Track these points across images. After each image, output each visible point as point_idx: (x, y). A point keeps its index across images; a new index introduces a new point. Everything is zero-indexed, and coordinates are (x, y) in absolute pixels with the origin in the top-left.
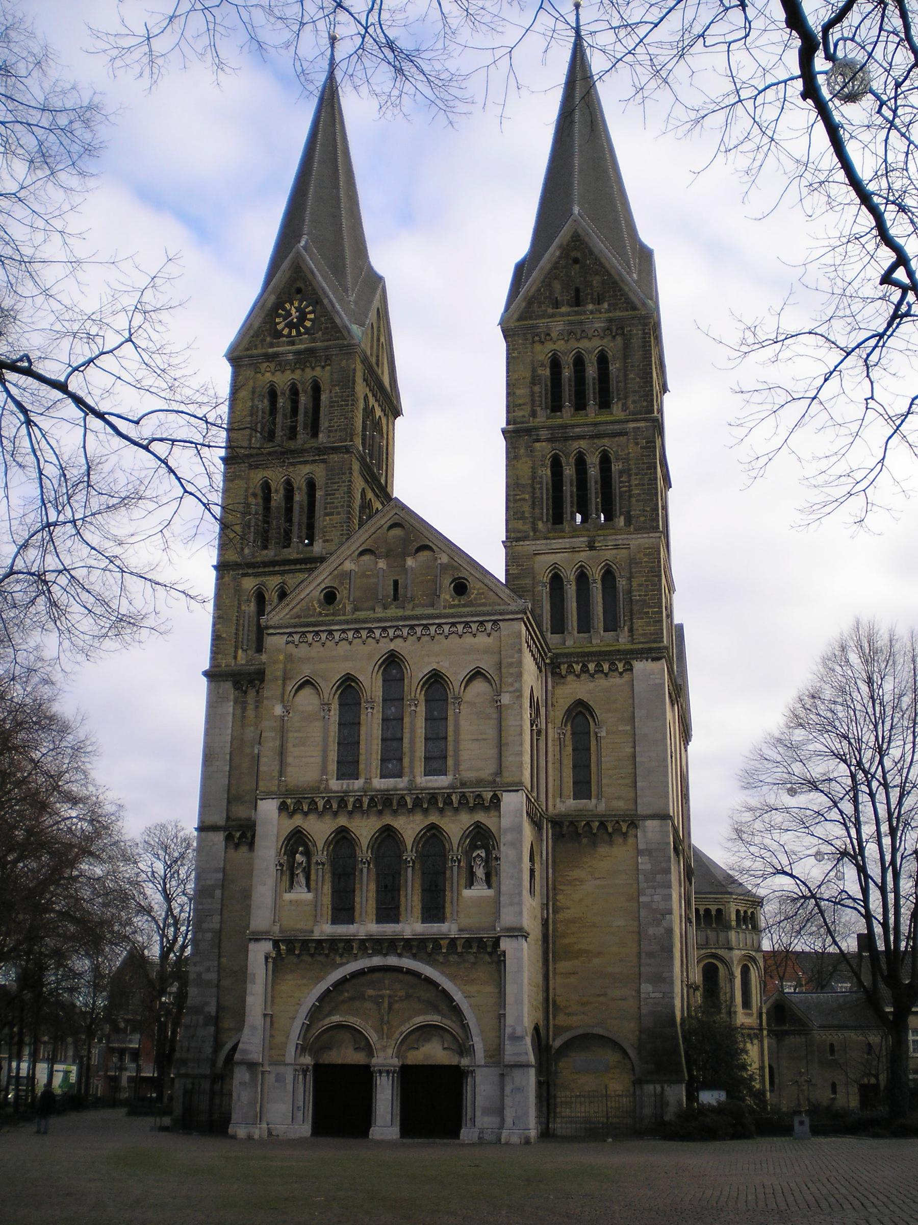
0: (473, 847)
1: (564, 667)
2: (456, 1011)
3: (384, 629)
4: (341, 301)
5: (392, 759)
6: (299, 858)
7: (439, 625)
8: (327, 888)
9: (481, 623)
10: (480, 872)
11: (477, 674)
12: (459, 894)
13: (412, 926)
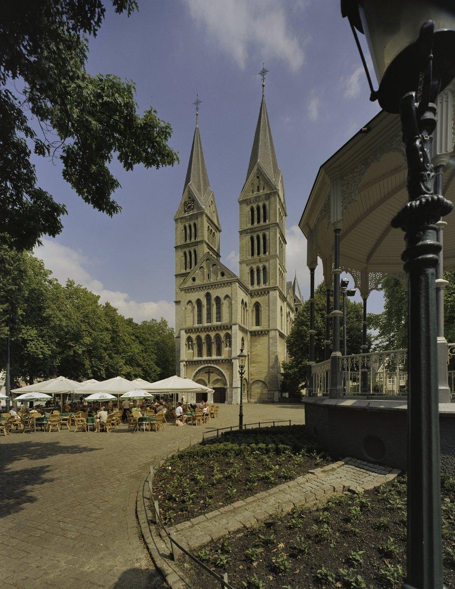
2: (224, 375)
4: (200, 199)
5: (209, 319)
6: (190, 343)
9: (227, 283)
10: (228, 344)
11: (227, 296)
13: (214, 357)
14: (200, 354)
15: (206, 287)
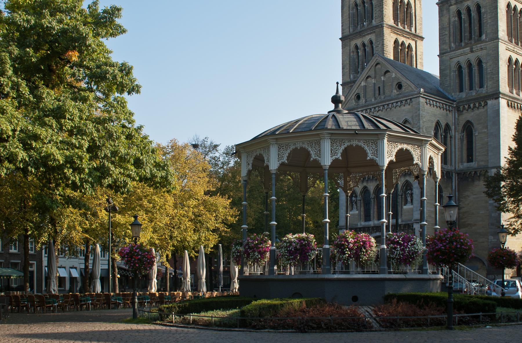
0: (407, 190)
1: (461, 107)
3: (375, 108)
7: (392, 103)
8: (362, 209)
9: (406, 100)
12: (402, 207)
14: (367, 218)
15: (375, 108)
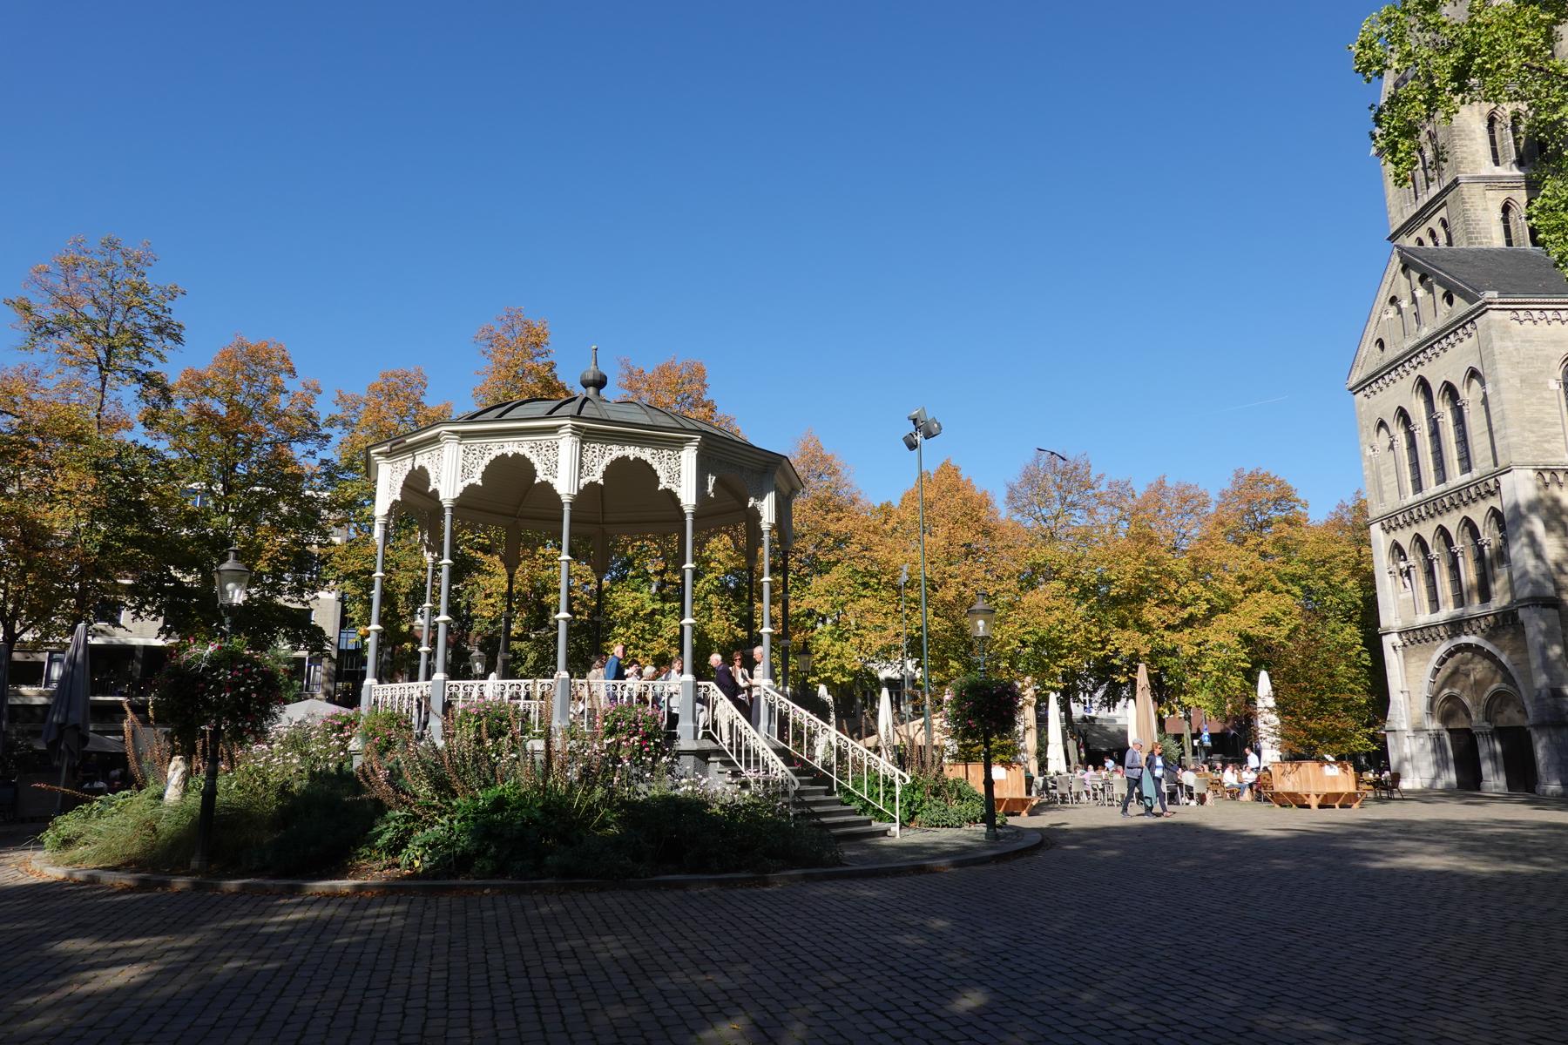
11: (1473, 374)
